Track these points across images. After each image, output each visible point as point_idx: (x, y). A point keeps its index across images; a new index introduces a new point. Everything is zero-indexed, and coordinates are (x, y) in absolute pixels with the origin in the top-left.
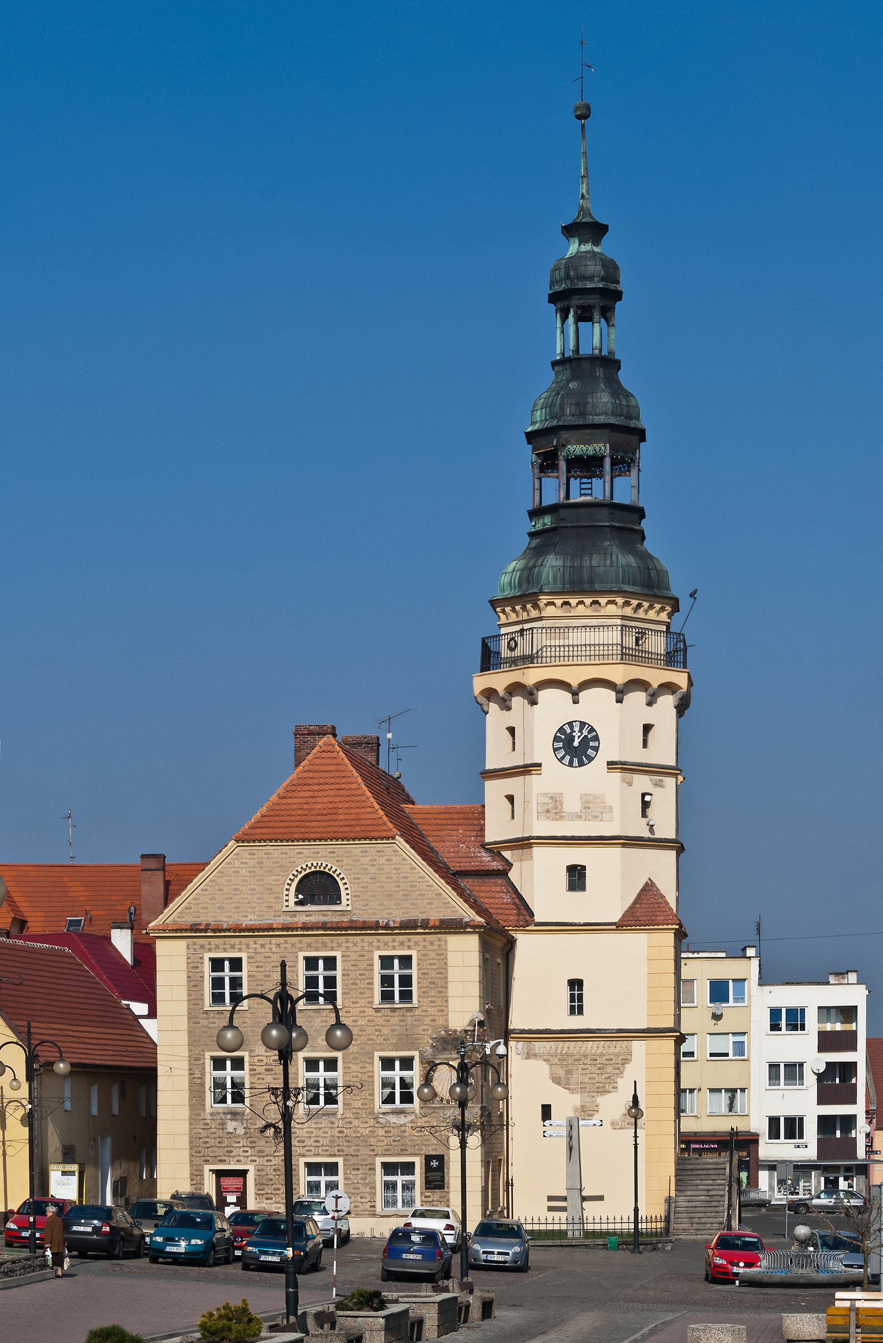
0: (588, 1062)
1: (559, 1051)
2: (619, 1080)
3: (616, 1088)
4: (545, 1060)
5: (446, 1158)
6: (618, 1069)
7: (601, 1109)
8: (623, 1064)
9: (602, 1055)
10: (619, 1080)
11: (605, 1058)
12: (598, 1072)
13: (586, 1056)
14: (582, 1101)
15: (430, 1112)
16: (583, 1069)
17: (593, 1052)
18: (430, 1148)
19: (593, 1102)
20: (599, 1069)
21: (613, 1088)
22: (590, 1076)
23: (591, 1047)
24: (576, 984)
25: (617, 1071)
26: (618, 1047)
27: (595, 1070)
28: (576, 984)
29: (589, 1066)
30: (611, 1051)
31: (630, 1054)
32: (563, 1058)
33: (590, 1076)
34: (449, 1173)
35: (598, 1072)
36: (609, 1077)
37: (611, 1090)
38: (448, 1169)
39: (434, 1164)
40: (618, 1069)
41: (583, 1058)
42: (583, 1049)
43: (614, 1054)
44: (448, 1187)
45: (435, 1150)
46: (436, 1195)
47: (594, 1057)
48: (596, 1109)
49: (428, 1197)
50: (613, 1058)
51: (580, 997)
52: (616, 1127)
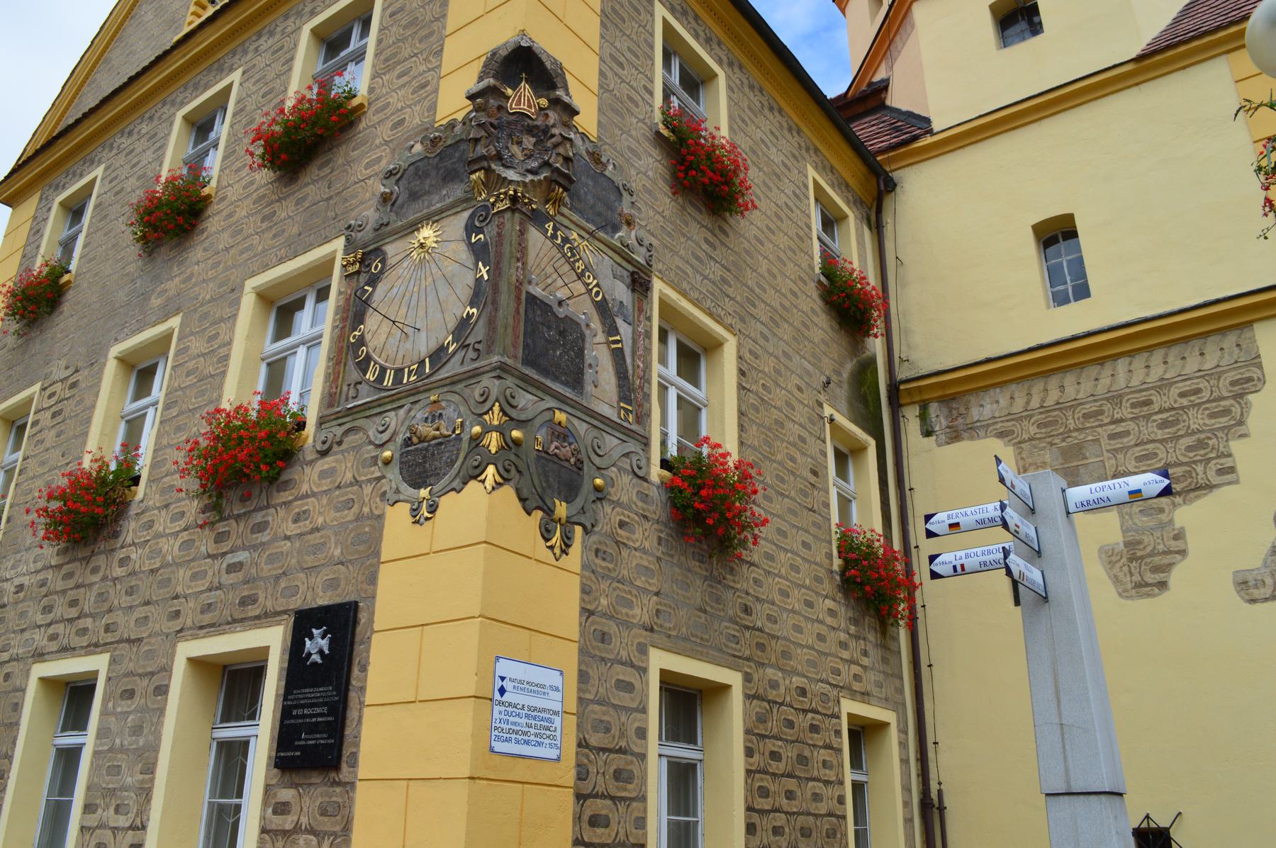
0: (1126, 412)
1: (1035, 403)
2: (1235, 446)
3: (1232, 470)
4: (1001, 435)
5: (363, 617)
6: (1226, 412)
7: (1192, 542)
8: (1239, 396)
9: (1163, 385)
10: (1235, 446)
11: (1174, 391)
12: (1160, 434)
13: (1116, 399)
14: (1125, 531)
15: (339, 431)
16: (1112, 437)
17: (1135, 382)
18: (319, 580)
19: (1162, 526)
20: (1164, 425)
21: (1221, 472)
22: (1138, 451)
23: (1127, 375)
24: (1057, 235)
25: (1223, 421)
26: (1215, 354)
27: (1151, 430)
28: (1057, 235)
29: (1131, 426)
30: (1191, 366)
31: (1256, 361)
32: (1049, 420)
33: (1138, 451)
34: (362, 689)
35: (1160, 434)
36: (1201, 444)
37: (1215, 480)
38: (364, 669)
39: (317, 644)
40: (1226, 412)
41: (1107, 407)
42: (1105, 381)
43: (1203, 374)
44: (354, 764)
45: (333, 584)
46: (307, 800)
47: (1142, 397)
48: (1175, 545)
49: (282, 809)
50: (1203, 384)
51: (1079, 268)
52: (1256, 593)
